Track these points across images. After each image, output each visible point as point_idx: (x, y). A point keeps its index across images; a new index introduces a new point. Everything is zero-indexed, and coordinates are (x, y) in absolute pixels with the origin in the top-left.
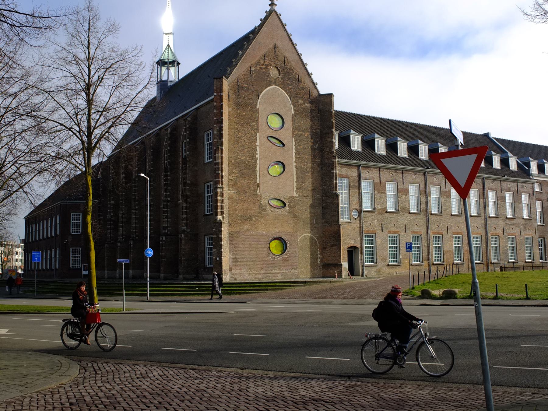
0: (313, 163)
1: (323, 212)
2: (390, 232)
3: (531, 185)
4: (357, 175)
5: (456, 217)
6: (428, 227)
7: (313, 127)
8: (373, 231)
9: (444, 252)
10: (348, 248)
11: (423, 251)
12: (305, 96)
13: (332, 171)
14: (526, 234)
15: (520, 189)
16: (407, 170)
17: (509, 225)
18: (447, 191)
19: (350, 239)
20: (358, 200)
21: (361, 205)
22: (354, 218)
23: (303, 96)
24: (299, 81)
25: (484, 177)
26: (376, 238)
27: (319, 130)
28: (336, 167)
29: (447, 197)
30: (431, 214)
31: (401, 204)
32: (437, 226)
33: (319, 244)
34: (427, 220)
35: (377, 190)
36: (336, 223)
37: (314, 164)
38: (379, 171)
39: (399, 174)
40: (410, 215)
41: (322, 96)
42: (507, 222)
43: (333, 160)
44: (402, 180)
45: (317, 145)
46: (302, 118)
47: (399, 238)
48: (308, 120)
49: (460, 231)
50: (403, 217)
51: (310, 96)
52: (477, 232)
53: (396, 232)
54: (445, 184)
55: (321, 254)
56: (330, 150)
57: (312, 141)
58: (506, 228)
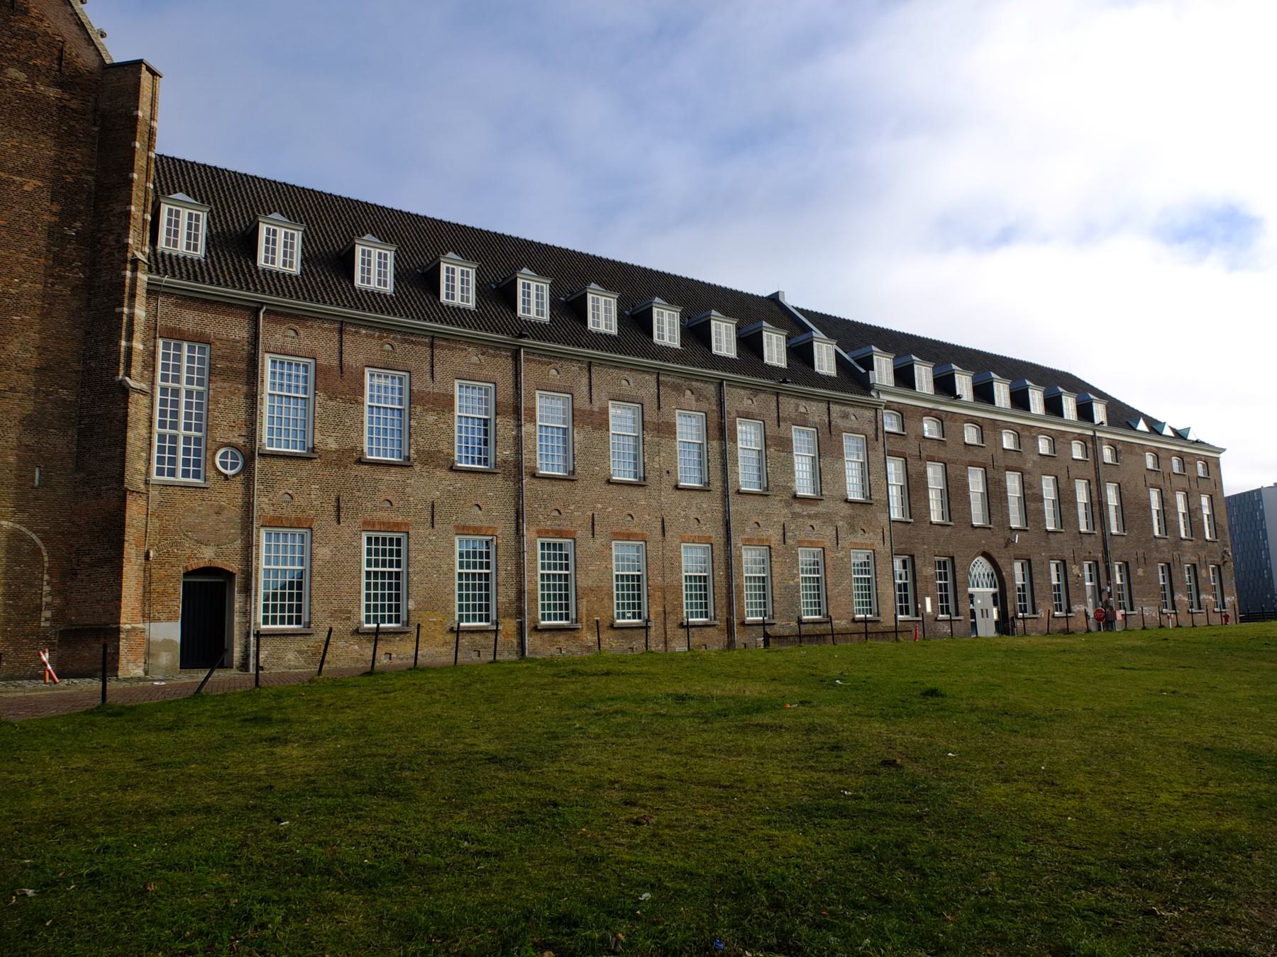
0: (50, 280)
1: (78, 446)
2: (368, 525)
3: (869, 414)
4: (246, 335)
5: (626, 488)
6: (519, 514)
7: (64, 165)
8: (298, 519)
9: (580, 592)
10: (187, 574)
11: (501, 589)
12: (38, 62)
13: (118, 310)
14: (855, 543)
15: (838, 421)
16: (448, 337)
17: (803, 516)
18: (596, 409)
19: (200, 542)
20: (243, 416)
21: (252, 434)
22: (220, 473)
23: (31, 58)
24: (13, 7)
25: (723, 380)
26: (312, 542)
27: (90, 178)
28: (133, 296)
29: (594, 429)
30: (534, 476)
31: (419, 439)
32: (556, 513)
33: (51, 556)
34: (519, 494)
35: (325, 391)
36: (115, 486)
37: (53, 284)
38: (341, 331)
39: (416, 348)
40: (452, 475)
41: (112, 70)
42: (797, 508)
43: (123, 273)
44: (427, 367)
45: (78, 224)
46: (17, 128)
47: (408, 545)
48: (42, 137)
49: (637, 530)
50: (426, 480)
51: (60, 65)
52: (696, 534)
53: (397, 524)
54: (591, 389)
55: (54, 593)
56: (117, 241)
57: (56, 208)
58: (793, 527)
